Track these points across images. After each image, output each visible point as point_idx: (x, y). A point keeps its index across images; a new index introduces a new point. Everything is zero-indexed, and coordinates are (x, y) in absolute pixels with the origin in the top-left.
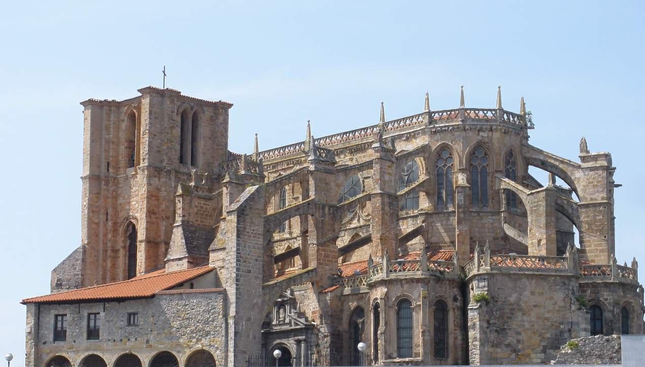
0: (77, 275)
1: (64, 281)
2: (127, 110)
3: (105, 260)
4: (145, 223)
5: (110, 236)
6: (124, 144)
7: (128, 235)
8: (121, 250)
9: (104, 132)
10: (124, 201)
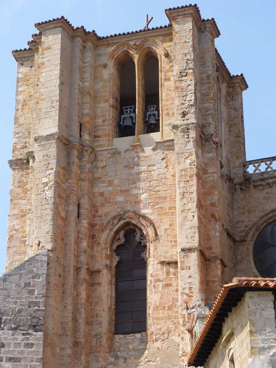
0: (36, 304)
1: (8, 315)
2: (114, 51)
3: (76, 285)
4: (196, 218)
5: (84, 244)
6: (107, 101)
7: (114, 247)
8: (105, 271)
9: (77, 76)
10: (110, 188)
